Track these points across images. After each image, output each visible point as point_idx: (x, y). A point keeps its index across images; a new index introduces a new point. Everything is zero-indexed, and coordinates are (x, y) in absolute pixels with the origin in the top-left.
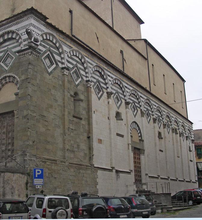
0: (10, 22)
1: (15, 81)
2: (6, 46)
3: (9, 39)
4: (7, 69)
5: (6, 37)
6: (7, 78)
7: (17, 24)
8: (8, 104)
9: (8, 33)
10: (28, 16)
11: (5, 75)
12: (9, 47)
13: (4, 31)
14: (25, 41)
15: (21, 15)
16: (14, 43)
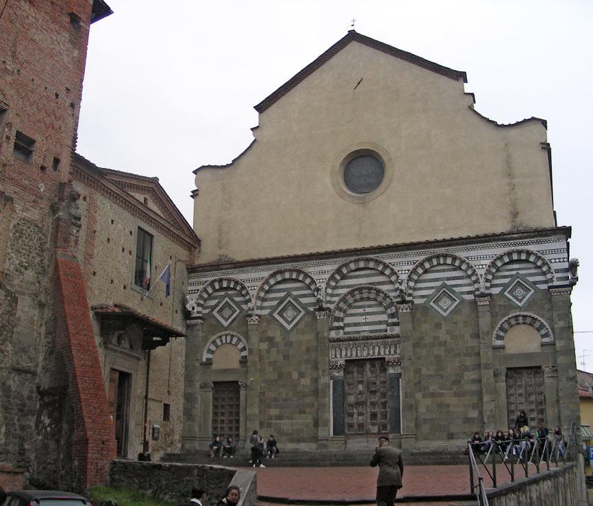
0: (533, 237)
1: (537, 325)
2: (513, 270)
3: (519, 261)
4: (520, 304)
5: (515, 257)
6: (521, 318)
7: (537, 243)
8: (530, 355)
9: (519, 252)
10: (559, 236)
11: (518, 314)
12: (520, 272)
13: (513, 248)
14: (557, 271)
15: (549, 232)
16: (530, 269)
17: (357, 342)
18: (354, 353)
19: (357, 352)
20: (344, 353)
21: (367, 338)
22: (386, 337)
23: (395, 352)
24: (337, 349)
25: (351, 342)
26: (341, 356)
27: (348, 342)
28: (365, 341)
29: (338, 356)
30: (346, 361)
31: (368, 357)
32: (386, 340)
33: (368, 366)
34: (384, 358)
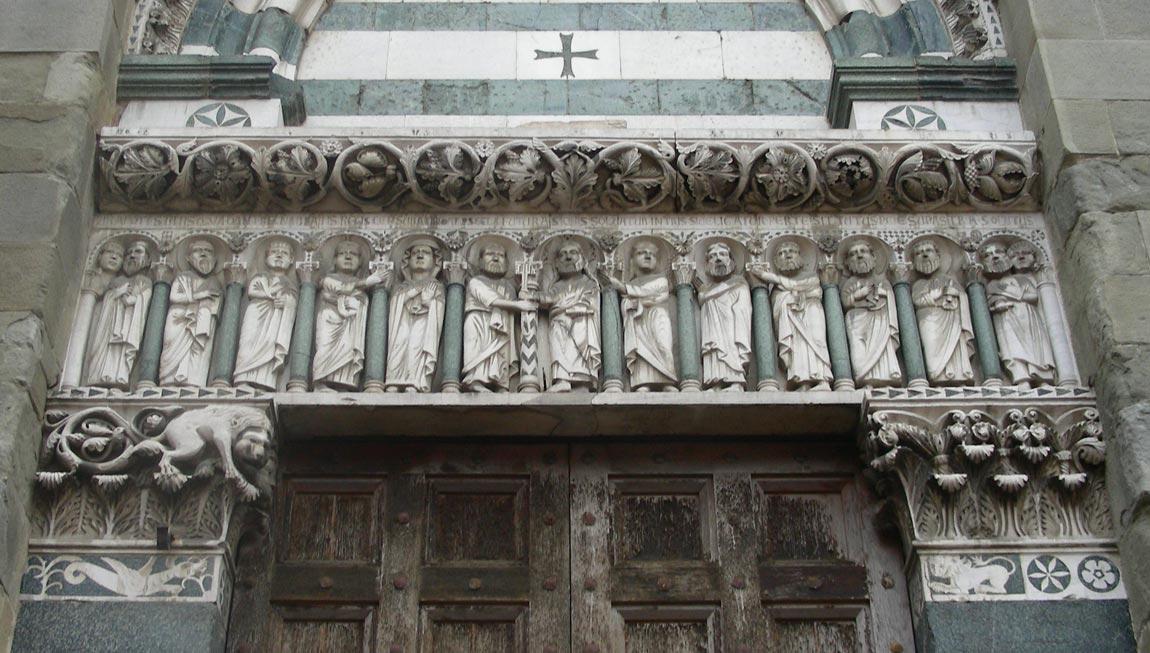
17: (475, 228)
18: (413, 340)
19: (449, 337)
20: (264, 334)
21: (611, 184)
22: (854, 185)
23: (986, 361)
24: (183, 289)
25: (376, 227)
26: (223, 369)
27: (327, 226)
28: (587, 228)
29: (186, 363)
30: (286, 420)
31: (613, 395)
32: (850, 226)
33: (591, 528)
34: (854, 413)
